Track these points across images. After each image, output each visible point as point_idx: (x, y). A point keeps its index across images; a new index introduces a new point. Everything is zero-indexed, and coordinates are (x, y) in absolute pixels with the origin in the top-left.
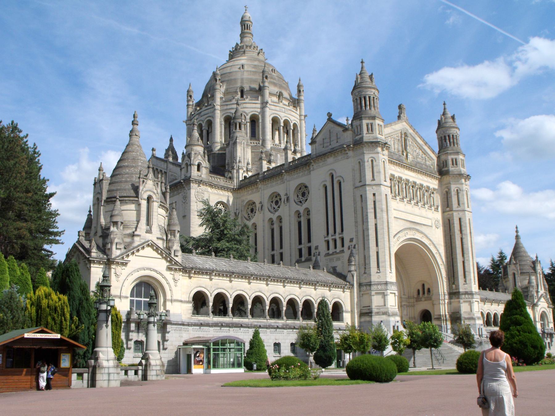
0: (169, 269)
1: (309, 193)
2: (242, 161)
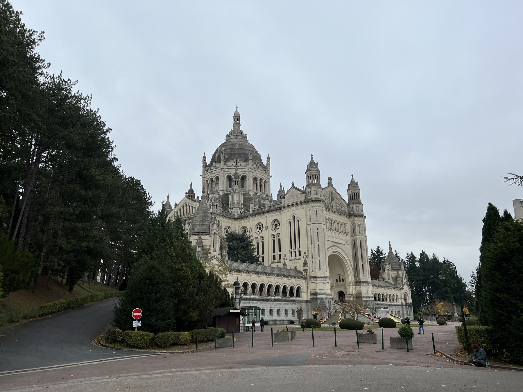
1: (280, 225)
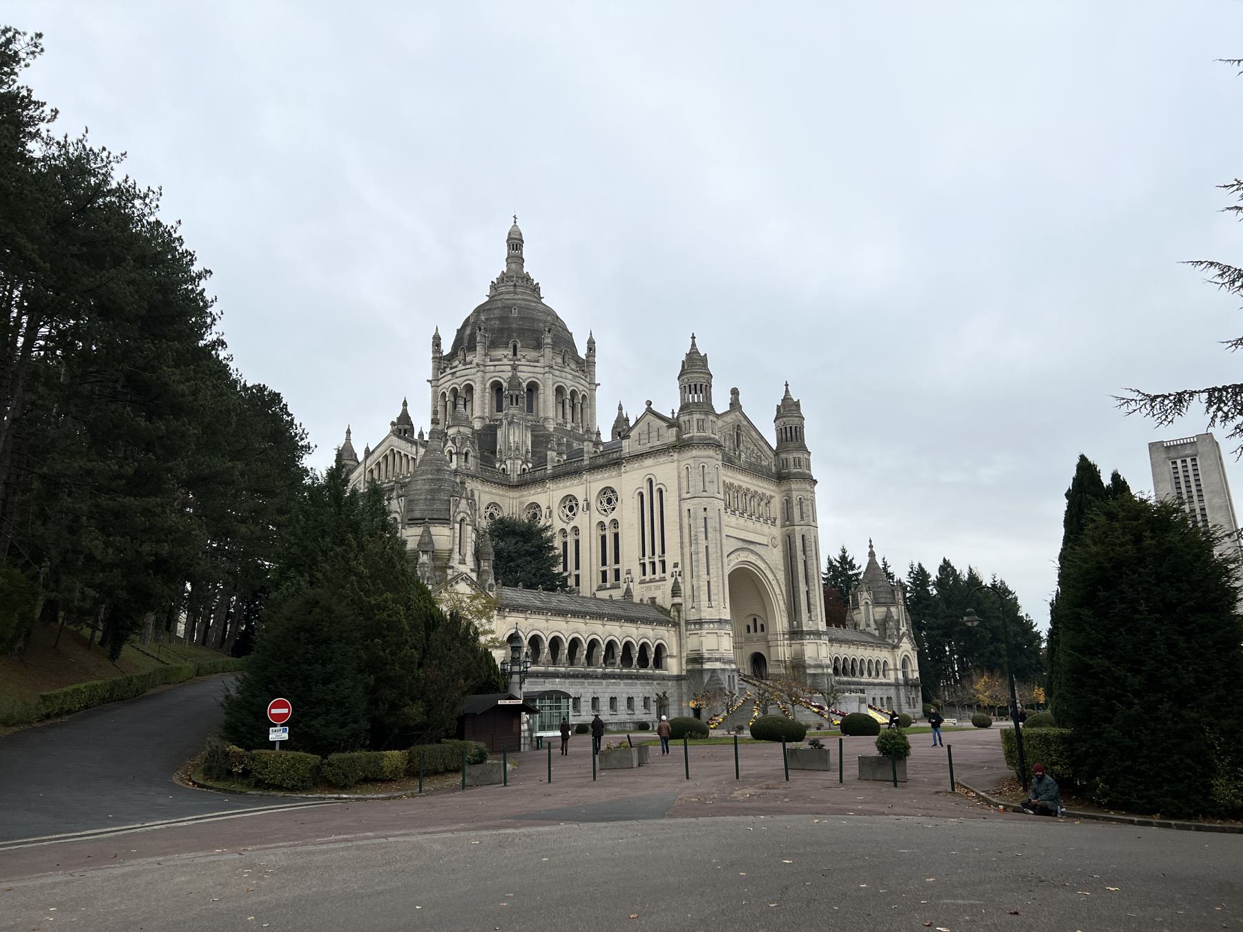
1: (617, 500)
2: (521, 448)
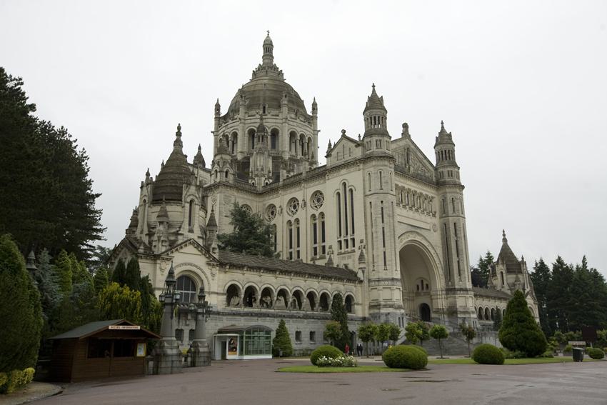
0: (208, 264)
